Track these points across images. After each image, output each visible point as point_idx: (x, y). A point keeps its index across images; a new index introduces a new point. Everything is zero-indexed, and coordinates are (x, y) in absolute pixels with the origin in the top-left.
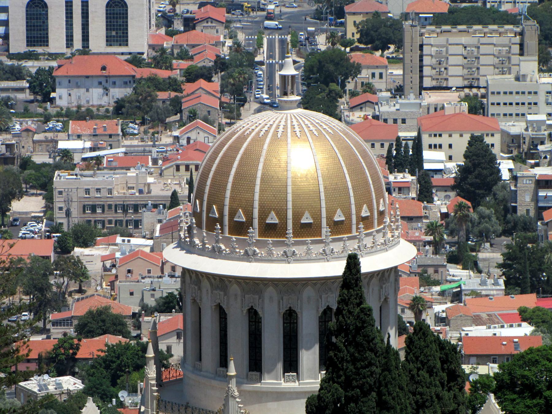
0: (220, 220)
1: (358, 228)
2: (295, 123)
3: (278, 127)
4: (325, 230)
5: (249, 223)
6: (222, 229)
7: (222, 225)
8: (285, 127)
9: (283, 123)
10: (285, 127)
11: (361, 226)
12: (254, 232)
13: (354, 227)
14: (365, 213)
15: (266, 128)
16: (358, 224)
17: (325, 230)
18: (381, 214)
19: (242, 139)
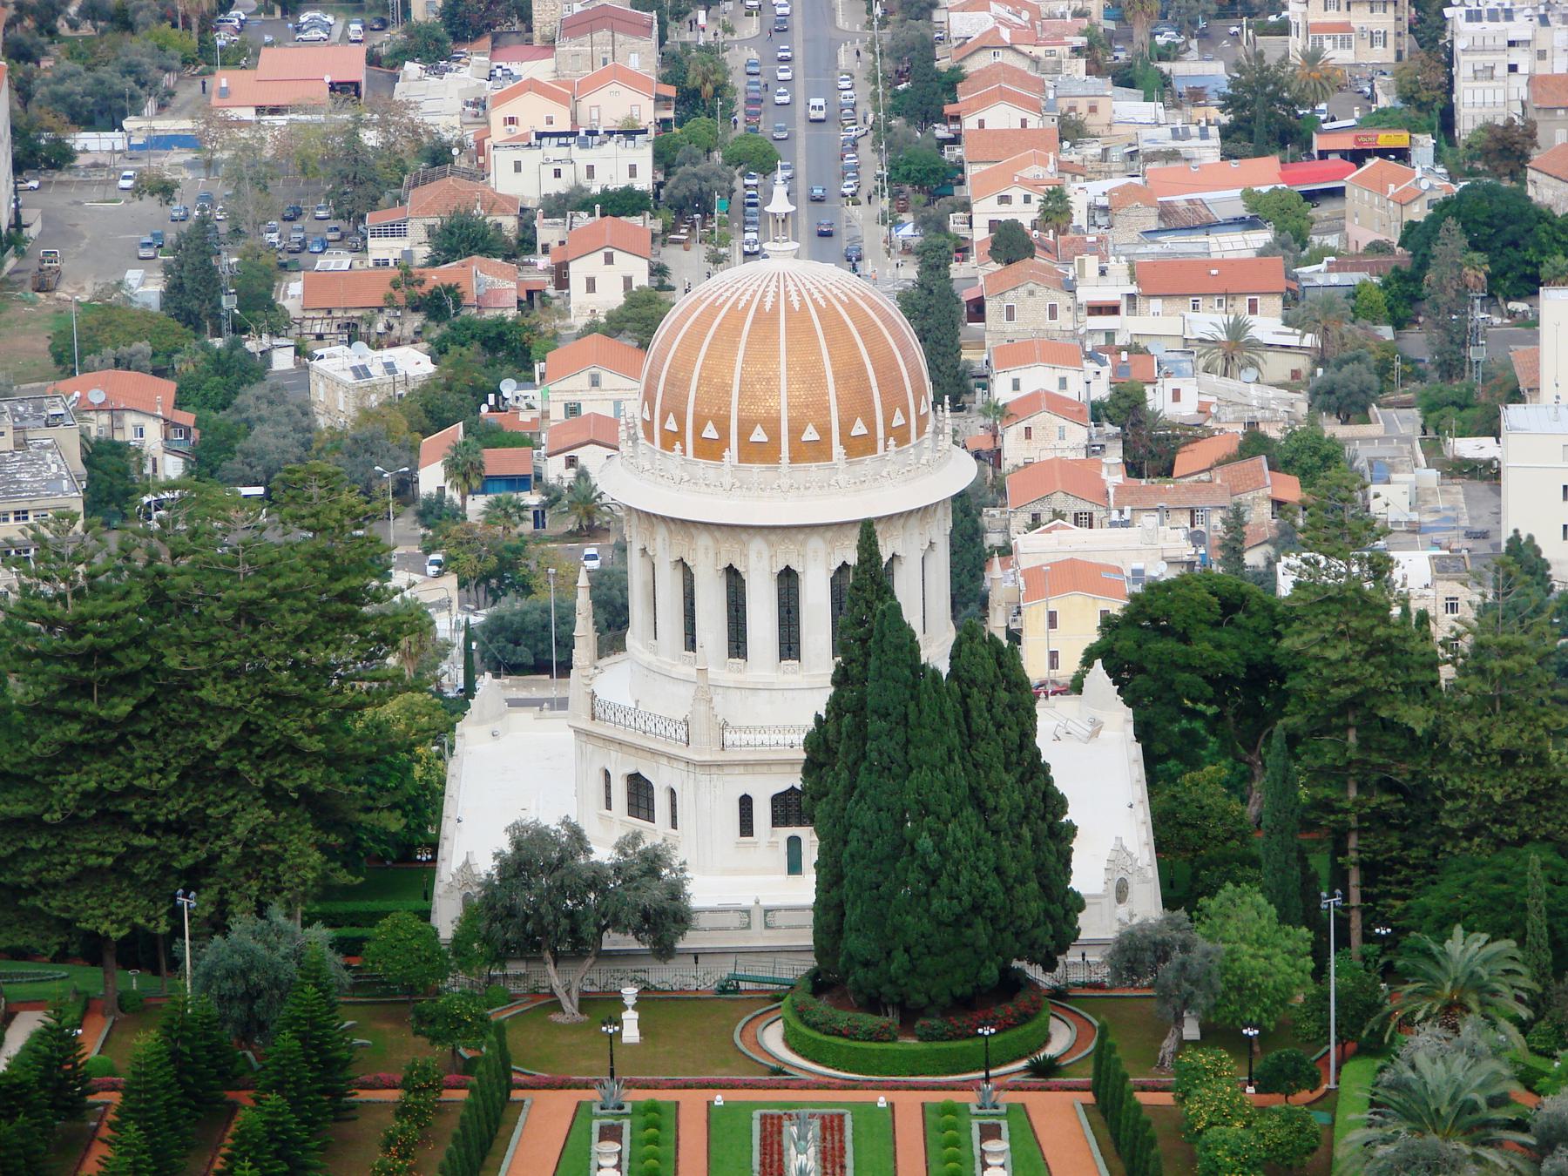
0: (679, 435)
1: (886, 446)
2: (791, 287)
3: (764, 295)
4: (838, 450)
5: (723, 441)
6: (684, 451)
7: (684, 445)
8: (777, 294)
9: (772, 288)
10: (777, 294)
11: (891, 441)
12: (731, 454)
13: (881, 444)
14: (898, 420)
15: (747, 296)
16: (886, 440)
17: (838, 450)
18: (922, 420)
19: (713, 310)
